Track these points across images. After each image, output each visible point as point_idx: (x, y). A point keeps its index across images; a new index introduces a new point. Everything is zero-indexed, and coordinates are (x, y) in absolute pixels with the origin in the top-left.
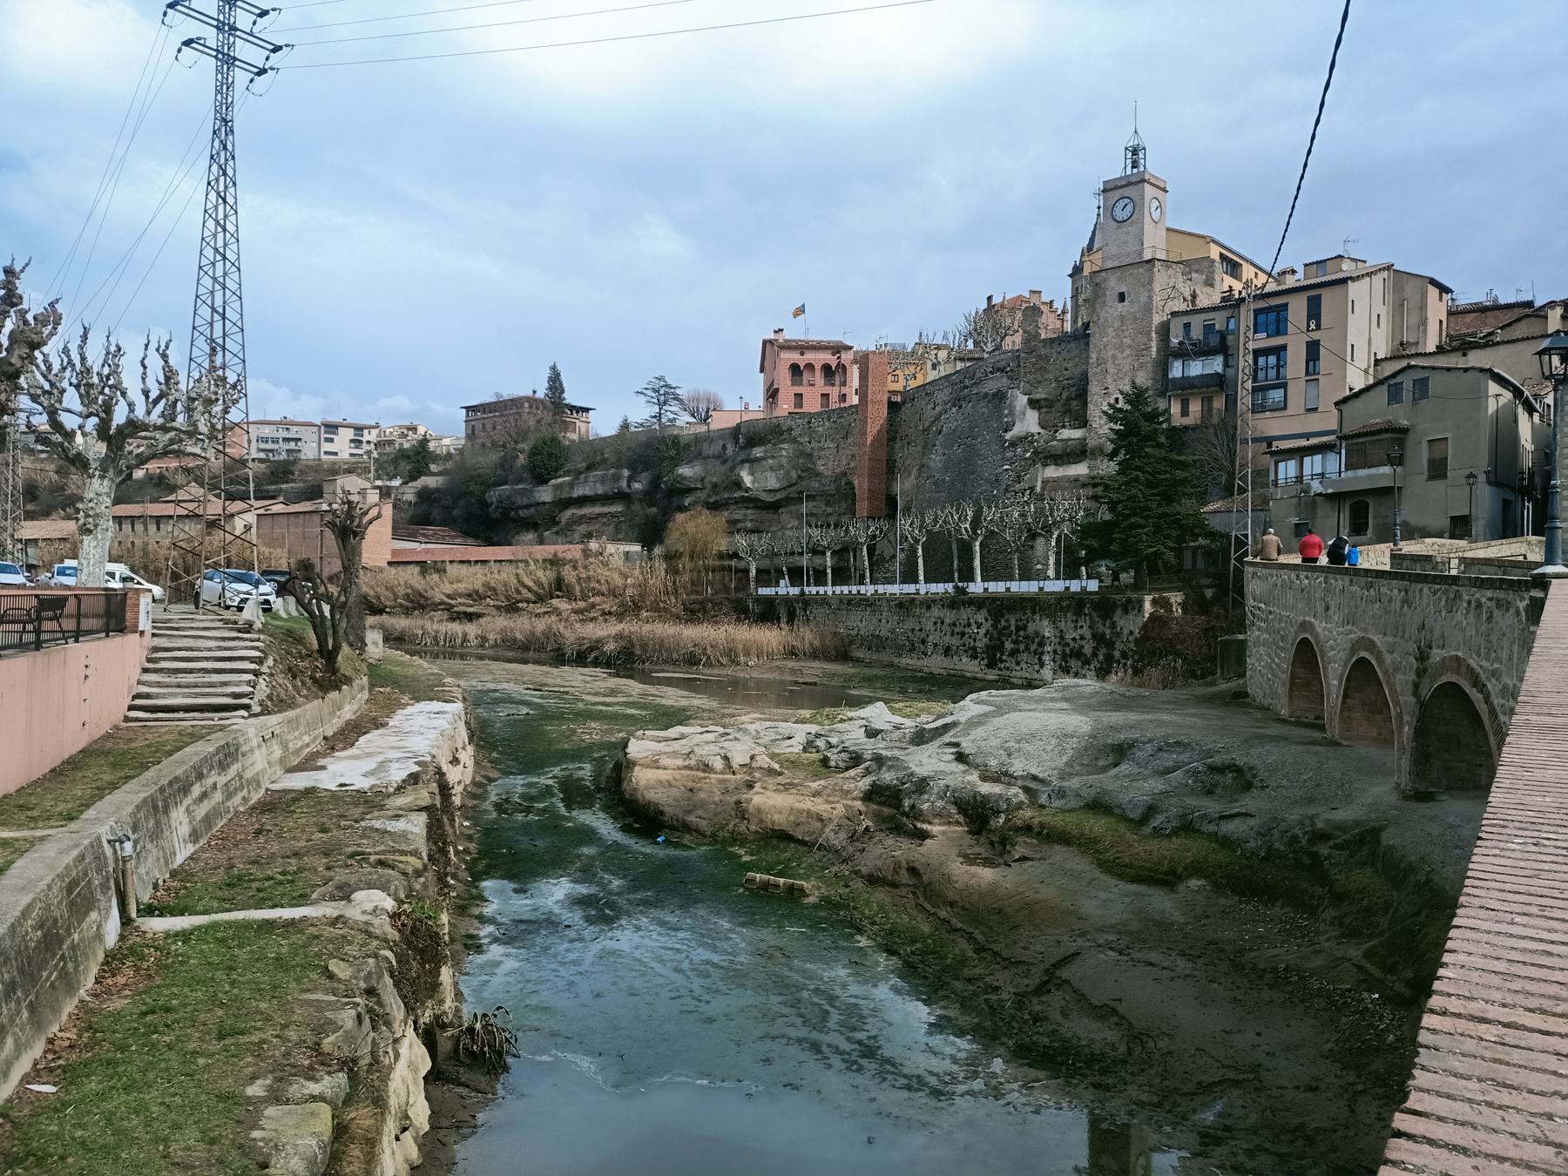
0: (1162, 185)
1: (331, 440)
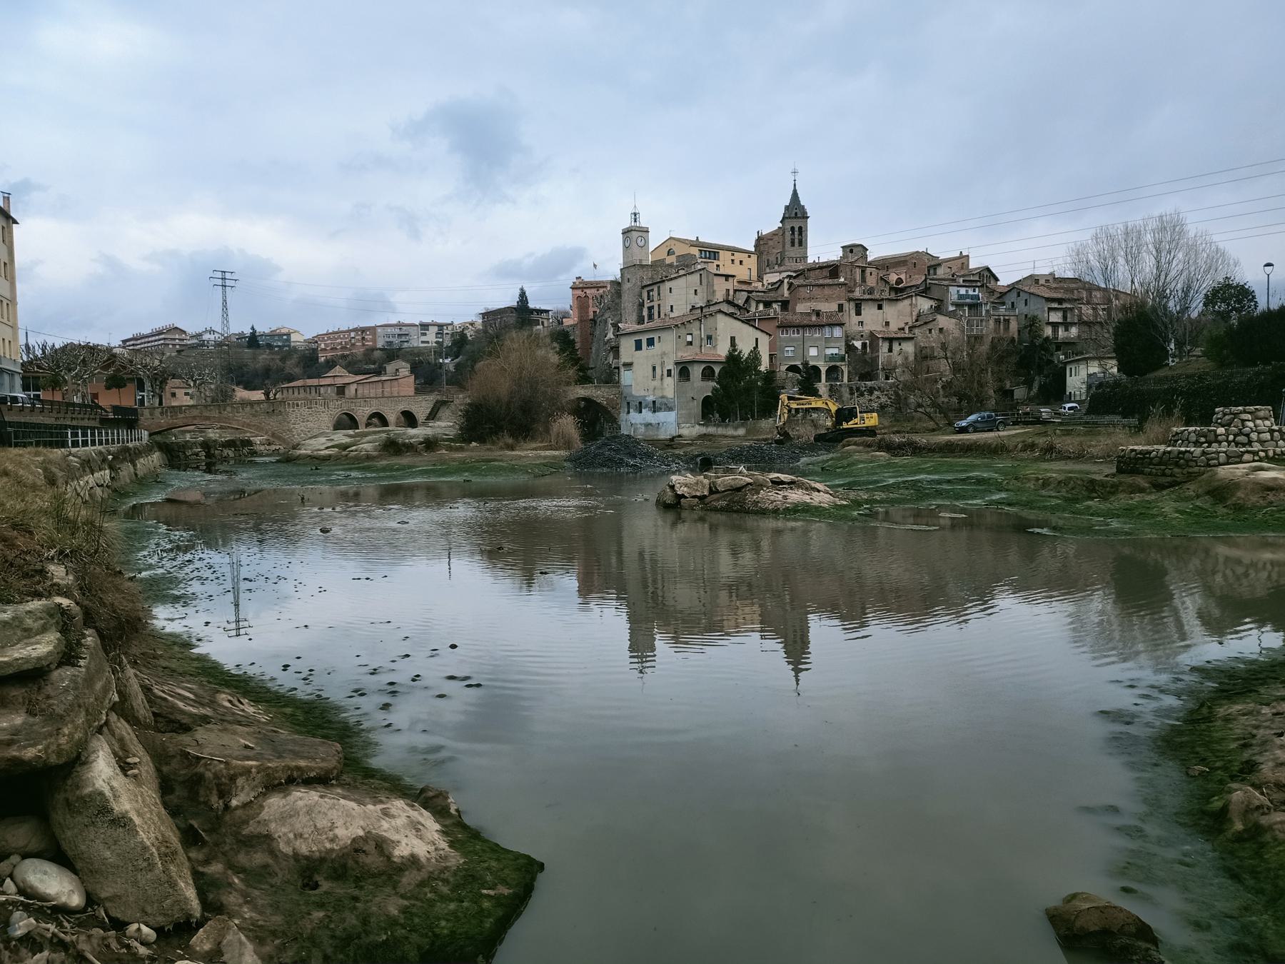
1: (425, 334)
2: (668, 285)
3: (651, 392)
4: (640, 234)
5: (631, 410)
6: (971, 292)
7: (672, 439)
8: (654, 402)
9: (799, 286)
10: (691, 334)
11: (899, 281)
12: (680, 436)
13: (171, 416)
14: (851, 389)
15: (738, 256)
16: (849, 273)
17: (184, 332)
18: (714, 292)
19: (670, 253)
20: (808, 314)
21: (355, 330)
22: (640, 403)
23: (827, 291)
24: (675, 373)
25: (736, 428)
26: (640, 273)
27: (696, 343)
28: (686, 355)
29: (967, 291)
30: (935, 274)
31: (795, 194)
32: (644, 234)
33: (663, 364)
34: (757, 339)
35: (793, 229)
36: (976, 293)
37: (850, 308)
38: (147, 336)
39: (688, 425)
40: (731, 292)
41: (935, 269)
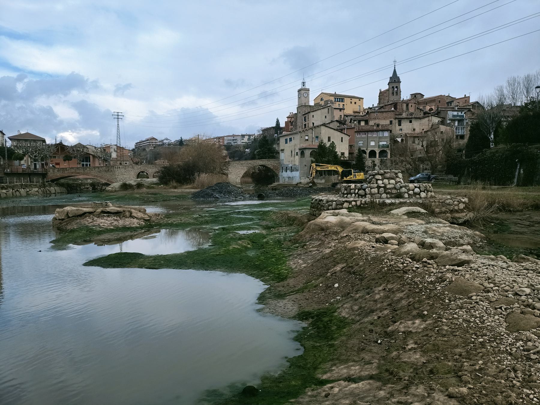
0: (308, 89)
1: (243, 139)
2: (312, 114)
3: (290, 163)
4: (305, 91)
5: (283, 171)
6: (460, 114)
7: (297, 184)
8: (291, 167)
9: (371, 113)
10: (308, 136)
11: (431, 109)
12: (300, 183)
13: (62, 172)
14: (391, 161)
15: (354, 100)
16: (401, 106)
17: (157, 140)
18: (334, 116)
19: (322, 100)
20: (373, 126)
21: (216, 138)
22: (287, 167)
23: (385, 114)
24: (299, 154)
25: (321, 180)
26: (304, 109)
27: (310, 140)
28: (305, 145)
29: (458, 113)
30: (451, 105)
31: (395, 71)
32: (307, 92)
33: (295, 149)
34: (342, 138)
35: (393, 87)
36: (463, 114)
37: (396, 122)
38: (144, 141)
39: (303, 178)
40: (343, 117)
41: (451, 103)
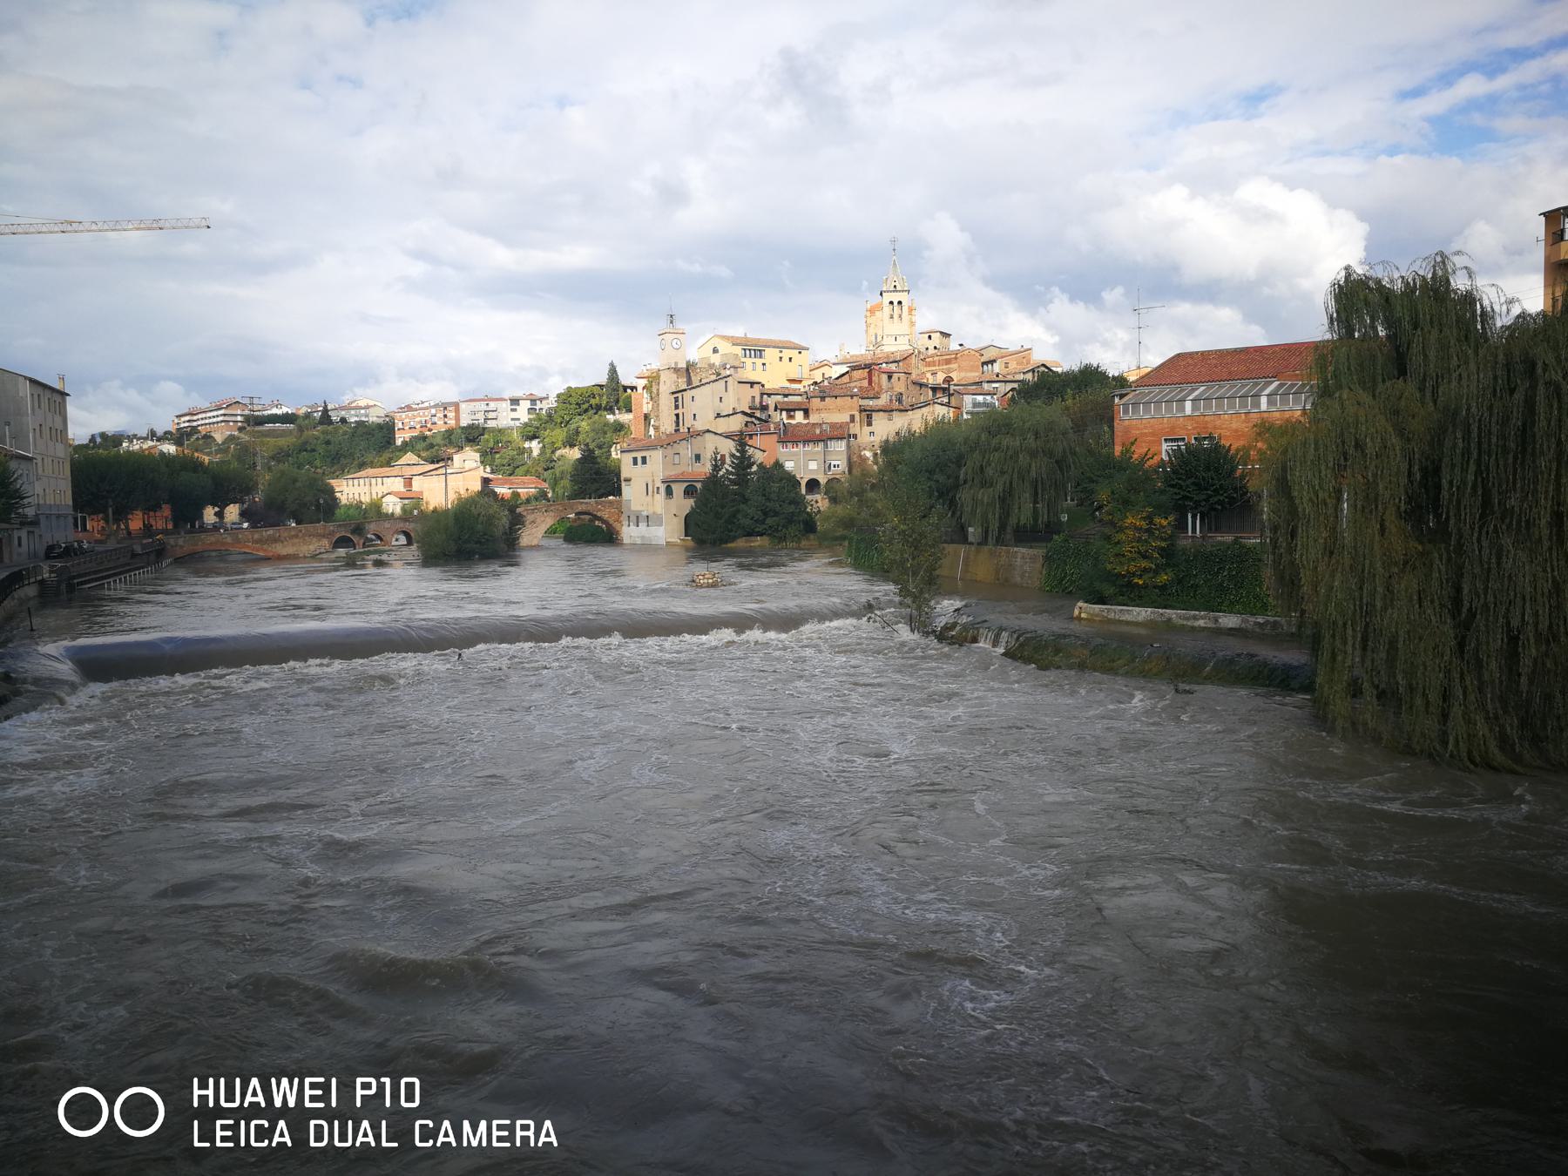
1: (514, 410)
15: (787, 353)
19: (715, 351)
